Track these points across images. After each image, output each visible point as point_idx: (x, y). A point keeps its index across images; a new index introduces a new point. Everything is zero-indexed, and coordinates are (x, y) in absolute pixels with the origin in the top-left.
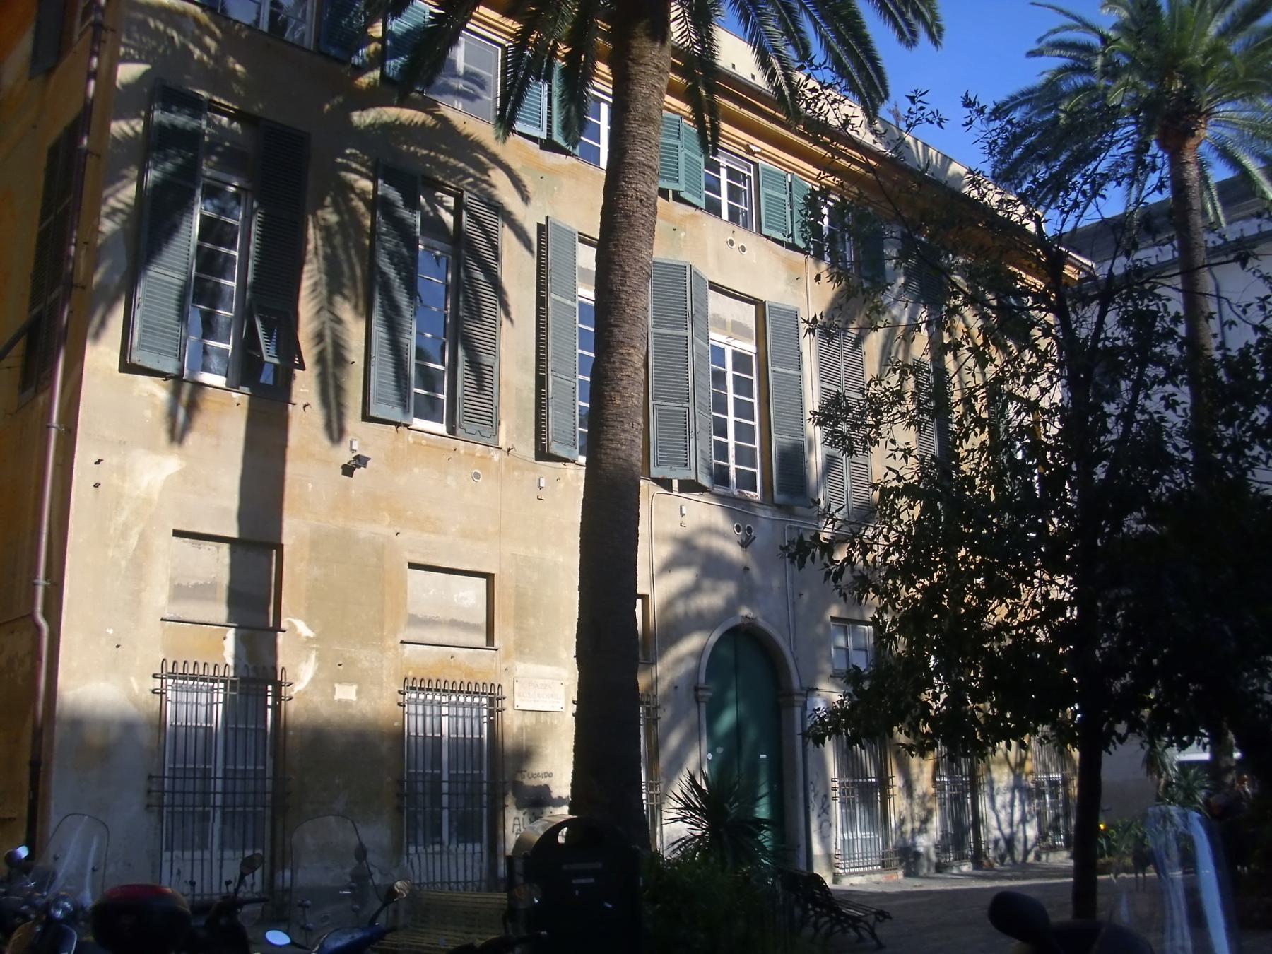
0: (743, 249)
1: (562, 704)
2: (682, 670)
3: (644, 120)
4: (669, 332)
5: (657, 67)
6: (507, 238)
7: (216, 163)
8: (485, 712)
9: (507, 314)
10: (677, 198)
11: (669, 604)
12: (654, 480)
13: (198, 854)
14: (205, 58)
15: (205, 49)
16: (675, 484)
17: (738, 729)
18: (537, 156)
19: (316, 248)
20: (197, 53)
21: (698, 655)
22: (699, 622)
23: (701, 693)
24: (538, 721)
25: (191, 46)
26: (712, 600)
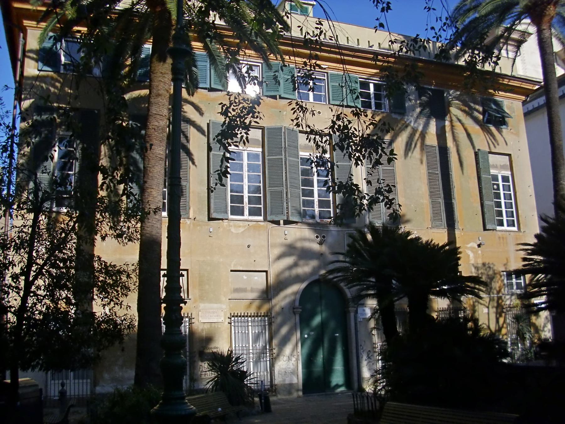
0: (319, 113)
1: (223, 319)
2: (288, 300)
3: (156, 96)
4: (274, 157)
5: (161, 73)
6: (192, 132)
7: (64, 129)
8: (187, 324)
9: (194, 163)
10: (281, 98)
11: (278, 275)
12: (269, 221)
13: (85, 381)
14: (56, 91)
15: (55, 87)
16: (282, 222)
17: (323, 325)
18: (206, 95)
19: (105, 153)
20: (52, 89)
21: (295, 293)
22: (298, 279)
23: (295, 310)
24: (211, 327)
25: (50, 88)
26: (305, 269)
